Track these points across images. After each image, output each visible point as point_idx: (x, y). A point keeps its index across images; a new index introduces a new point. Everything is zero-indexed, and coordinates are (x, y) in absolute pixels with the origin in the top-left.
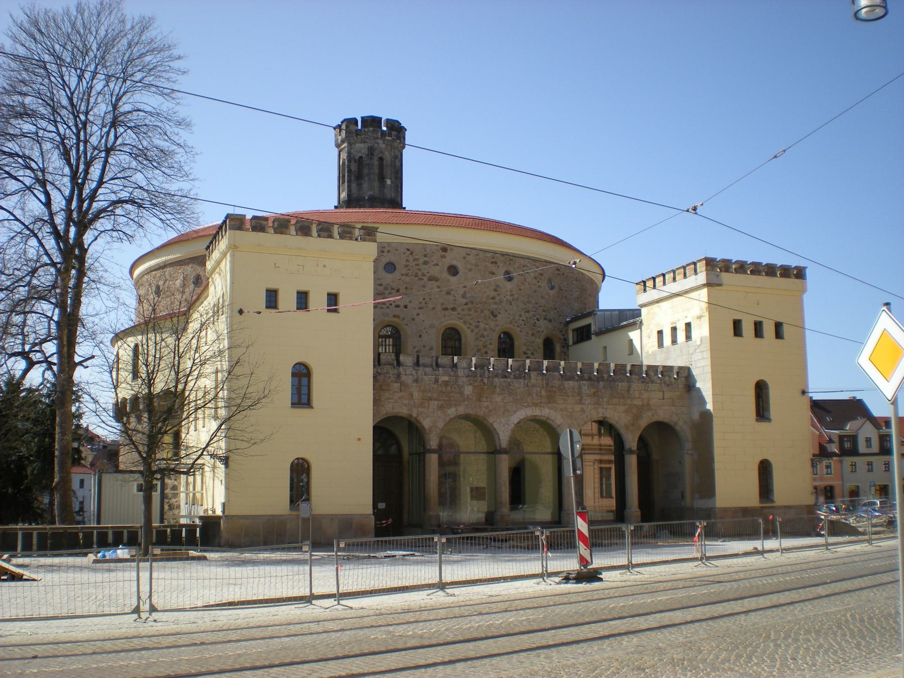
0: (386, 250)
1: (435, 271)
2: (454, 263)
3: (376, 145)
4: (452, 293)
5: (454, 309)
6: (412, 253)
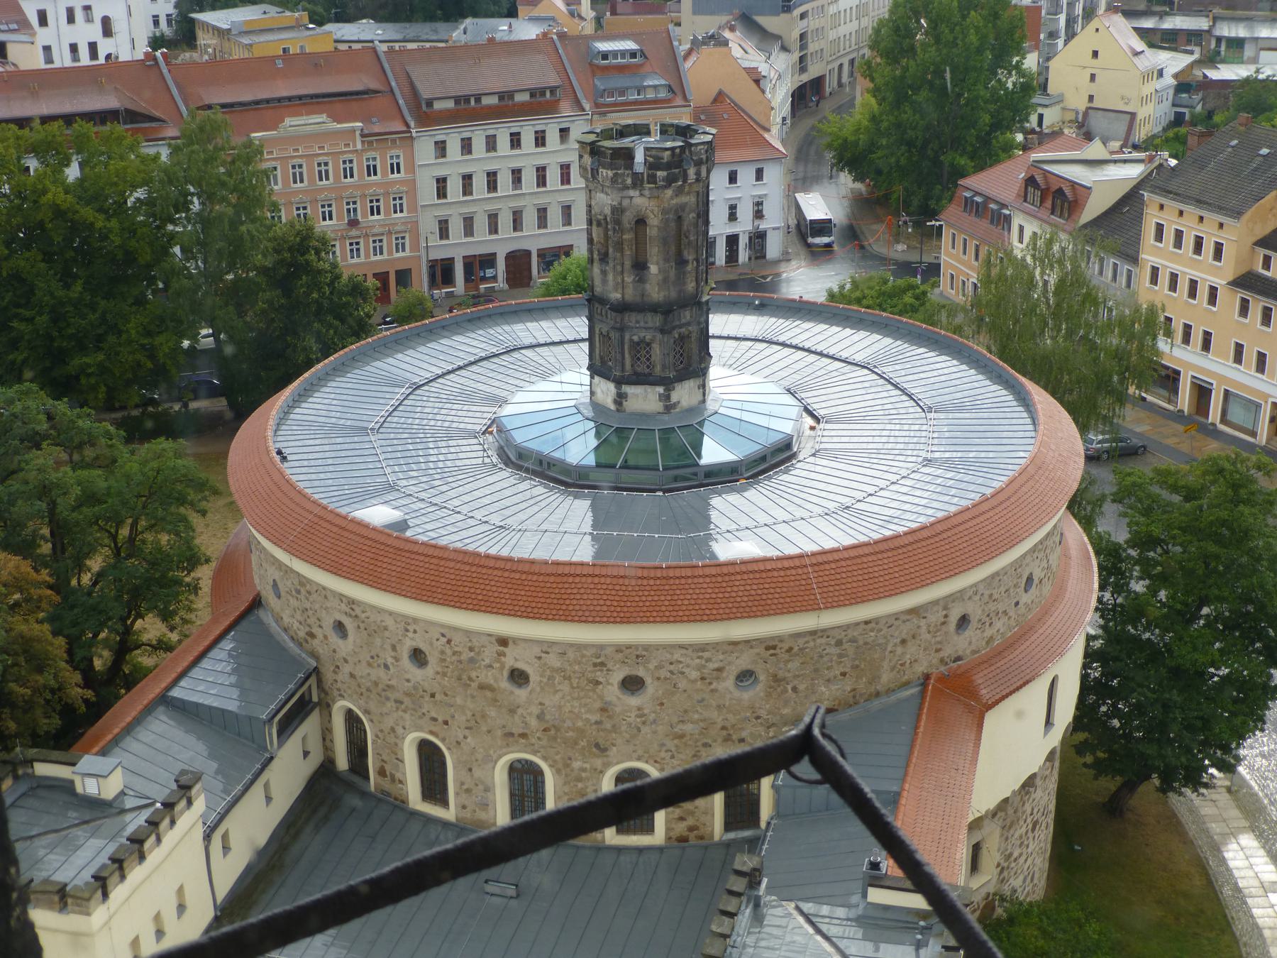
0: (411, 628)
1: (488, 677)
2: (521, 665)
3: (626, 203)
4: (520, 711)
5: (523, 736)
6: (449, 642)
